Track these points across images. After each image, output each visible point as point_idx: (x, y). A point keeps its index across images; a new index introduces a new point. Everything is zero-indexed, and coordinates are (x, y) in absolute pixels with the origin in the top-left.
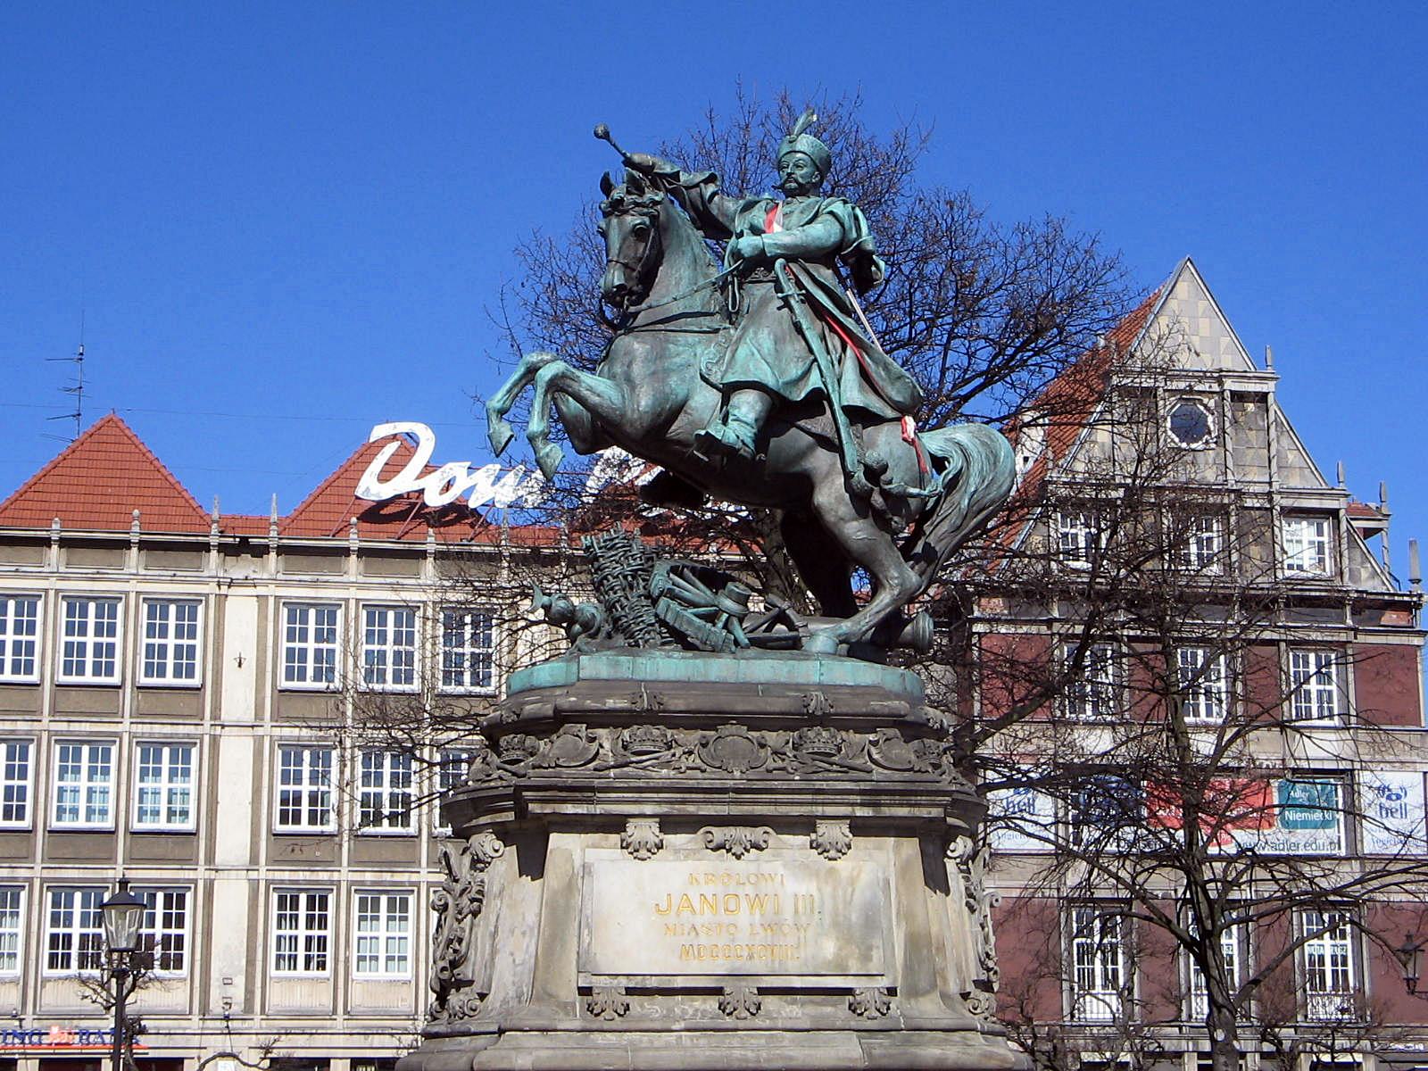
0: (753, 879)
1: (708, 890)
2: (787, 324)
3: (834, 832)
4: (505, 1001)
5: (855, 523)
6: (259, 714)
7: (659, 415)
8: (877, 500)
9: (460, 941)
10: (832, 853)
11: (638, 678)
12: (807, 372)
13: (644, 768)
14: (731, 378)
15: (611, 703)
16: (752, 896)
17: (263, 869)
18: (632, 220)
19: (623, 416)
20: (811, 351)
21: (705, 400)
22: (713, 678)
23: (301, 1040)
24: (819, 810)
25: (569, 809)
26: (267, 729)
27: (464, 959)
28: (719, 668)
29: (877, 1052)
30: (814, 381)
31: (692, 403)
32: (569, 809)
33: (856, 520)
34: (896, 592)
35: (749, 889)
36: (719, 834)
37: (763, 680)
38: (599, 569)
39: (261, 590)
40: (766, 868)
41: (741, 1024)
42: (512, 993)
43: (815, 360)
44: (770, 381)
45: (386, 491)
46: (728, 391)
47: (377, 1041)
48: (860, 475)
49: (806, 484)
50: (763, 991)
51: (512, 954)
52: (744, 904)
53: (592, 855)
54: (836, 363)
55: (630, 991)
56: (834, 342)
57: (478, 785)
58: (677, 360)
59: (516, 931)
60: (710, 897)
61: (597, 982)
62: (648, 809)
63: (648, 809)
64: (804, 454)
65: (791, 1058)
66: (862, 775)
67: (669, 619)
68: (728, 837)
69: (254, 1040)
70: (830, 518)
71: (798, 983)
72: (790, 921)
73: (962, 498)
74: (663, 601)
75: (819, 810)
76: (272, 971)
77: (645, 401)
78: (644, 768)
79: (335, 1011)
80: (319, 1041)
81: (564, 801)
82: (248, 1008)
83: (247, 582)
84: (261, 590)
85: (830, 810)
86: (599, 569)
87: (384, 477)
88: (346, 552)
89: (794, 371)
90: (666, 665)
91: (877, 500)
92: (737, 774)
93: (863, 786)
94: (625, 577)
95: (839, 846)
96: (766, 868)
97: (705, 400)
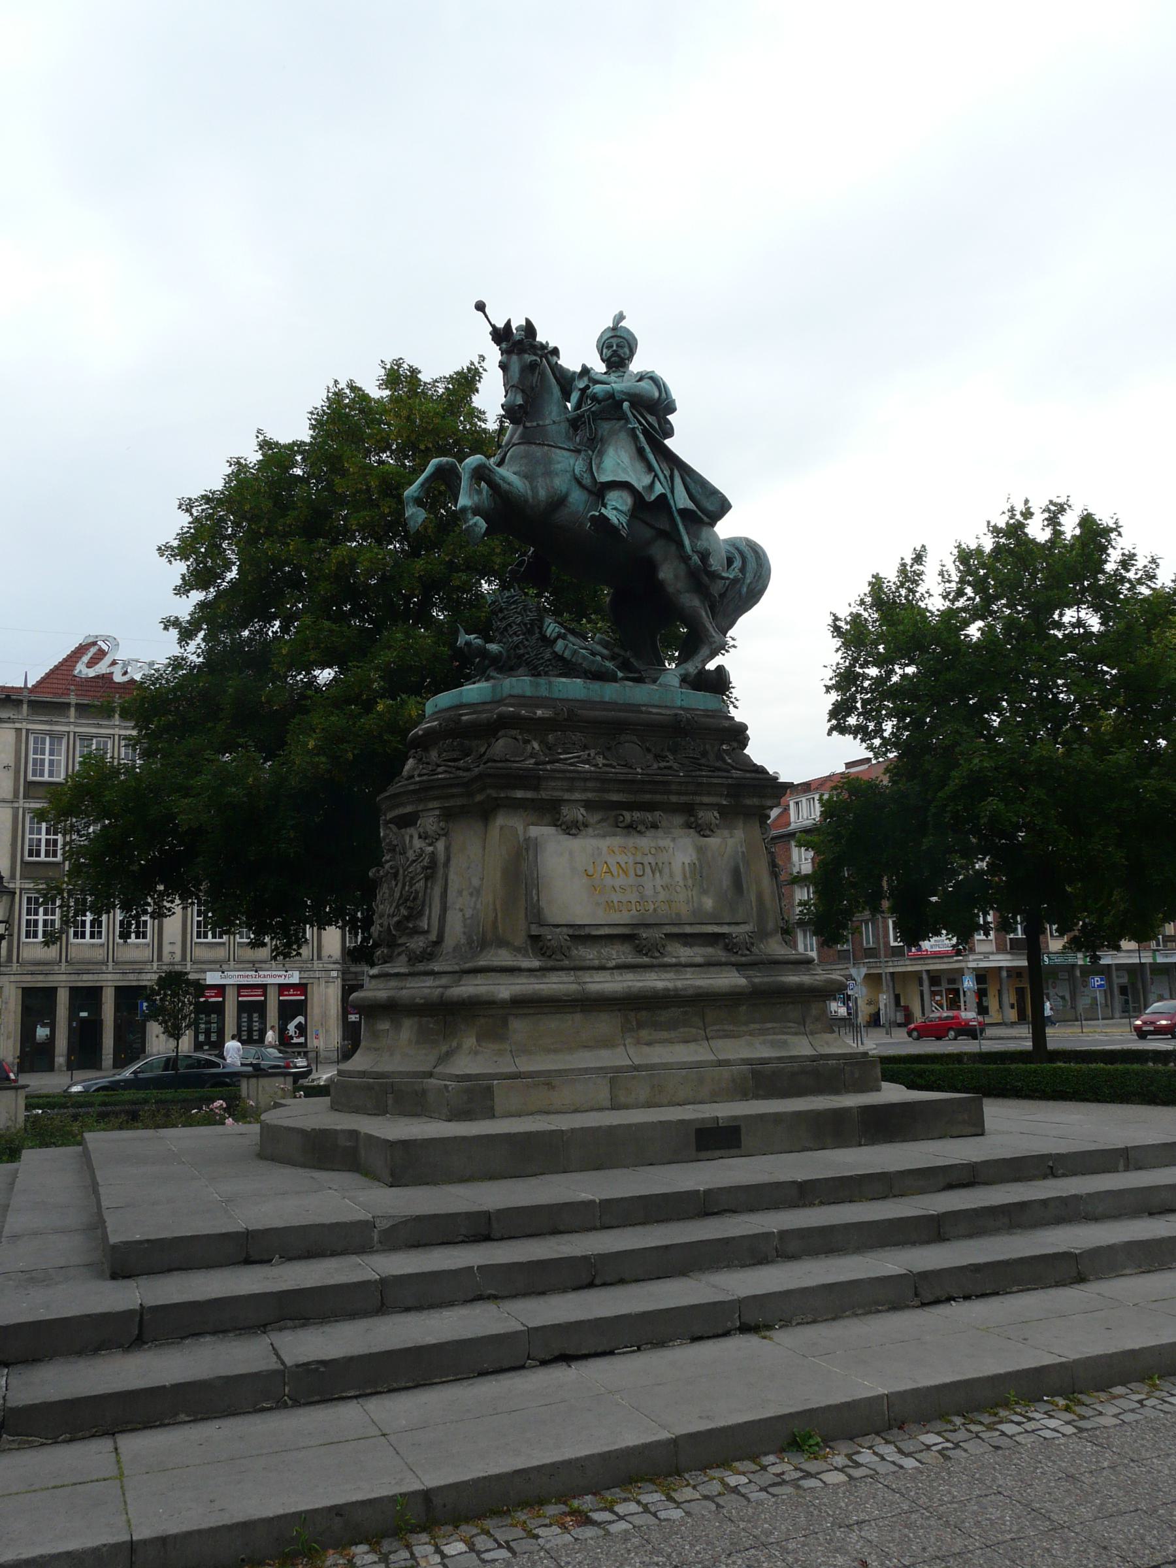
0: (653, 851)
1: (622, 859)
3: (712, 816)
4: (457, 948)
5: (687, 595)
6: (16, 795)
9: (415, 899)
11: (556, 695)
12: (653, 483)
13: (571, 764)
14: (603, 478)
15: (539, 712)
16: (653, 864)
17: (18, 882)
18: (528, 358)
19: (526, 501)
20: (650, 468)
21: (577, 497)
22: (607, 699)
23: (41, 978)
24: (698, 799)
25: (519, 794)
26: (21, 803)
27: (421, 914)
28: (610, 691)
29: (756, 980)
30: (659, 489)
31: (571, 499)
32: (519, 794)
35: (650, 858)
36: (628, 816)
38: (504, 618)
39: (18, 725)
40: (662, 843)
41: (655, 961)
42: (463, 941)
43: (656, 476)
44: (636, 485)
45: (91, 673)
46: (599, 491)
47: (85, 977)
48: (696, 558)
49: (651, 567)
50: (669, 936)
51: (461, 910)
52: (648, 870)
53: (535, 831)
55: (573, 937)
56: (665, 466)
57: (424, 778)
58: (559, 466)
59: (465, 893)
60: (623, 865)
61: (543, 931)
62: (577, 796)
63: (577, 796)
65: (700, 987)
66: (725, 774)
67: (567, 654)
68: (635, 818)
69: (13, 978)
70: (671, 589)
71: (688, 930)
72: (681, 883)
74: (560, 642)
75: (698, 799)
76: (23, 939)
77: (542, 493)
78: (571, 764)
79: (60, 961)
80: (51, 978)
81: (515, 787)
82: (9, 959)
83: (9, 720)
84: (18, 725)
86: (504, 618)
87: (90, 665)
88: (68, 705)
89: (647, 480)
90: (572, 688)
91: (705, 579)
92: (639, 770)
93: (730, 781)
94: (525, 625)
96: (662, 843)
97: (577, 497)
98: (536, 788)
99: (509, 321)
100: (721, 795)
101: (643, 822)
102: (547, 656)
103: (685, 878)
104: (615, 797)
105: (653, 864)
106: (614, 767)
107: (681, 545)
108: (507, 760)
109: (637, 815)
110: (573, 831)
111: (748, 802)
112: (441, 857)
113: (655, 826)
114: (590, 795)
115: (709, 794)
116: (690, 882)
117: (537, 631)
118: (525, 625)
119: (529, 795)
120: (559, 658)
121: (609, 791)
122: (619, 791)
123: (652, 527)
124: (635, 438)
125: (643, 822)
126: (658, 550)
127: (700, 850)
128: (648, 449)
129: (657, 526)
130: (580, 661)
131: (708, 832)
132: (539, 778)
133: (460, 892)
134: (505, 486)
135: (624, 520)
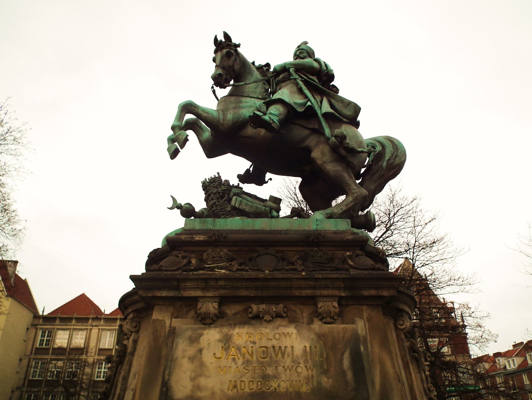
0: (277, 336)
2: (295, 89)
3: (330, 306)
7: (236, 122)
8: (343, 152)
10: (328, 319)
19: (218, 121)
20: (306, 97)
24: (318, 292)
32: (164, 294)
33: (332, 162)
34: (355, 196)
35: (274, 342)
36: (255, 308)
37: (284, 229)
54: (319, 103)
58: (247, 104)
64: (305, 139)
67: (237, 205)
68: (261, 309)
70: (319, 162)
73: (383, 162)
74: (234, 198)
75: (318, 292)
81: (160, 289)
85: (325, 292)
92: (267, 272)
95: (332, 315)
98: (177, 288)
99: (216, 36)
100: (339, 288)
101: (268, 313)
102: (229, 209)
103: (306, 361)
104: (243, 293)
105: (277, 348)
106: (247, 271)
107: (323, 134)
108: (159, 270)
109: (263, 307)
110: (208, 321)
111: (366, 293)
112: (129, 349)
113: (279, 316)
114: (222, 292)
115: (326, 288)
116: (310, 364)
117: (227, 196)
118: (219, 193)
119: (171, 294)
120: (234, 208)
121: (239, 288)
122: (247, 288)
123: (307, 128)
124: (297, 84)
125: (268, 313)
126: (312, 141)
127: (320, 336)
128: (304, 88)
129: (310, 127)
130: (244, 207)
131: (328, 319)
132: (178, 280)
133: (135, 376)
134: (204, 115)
135: (275, 119)
